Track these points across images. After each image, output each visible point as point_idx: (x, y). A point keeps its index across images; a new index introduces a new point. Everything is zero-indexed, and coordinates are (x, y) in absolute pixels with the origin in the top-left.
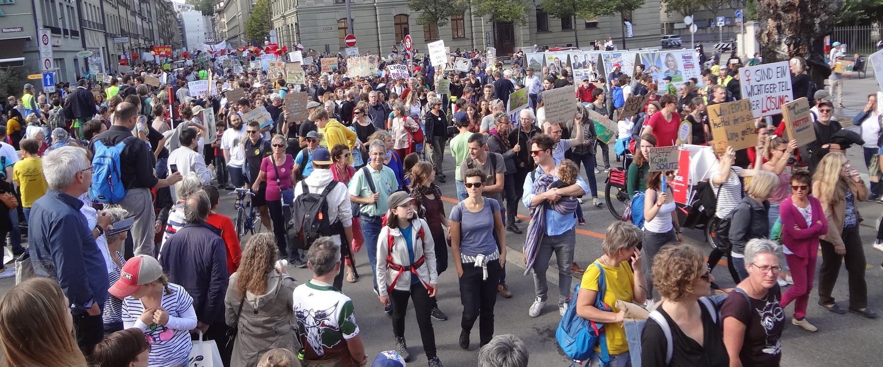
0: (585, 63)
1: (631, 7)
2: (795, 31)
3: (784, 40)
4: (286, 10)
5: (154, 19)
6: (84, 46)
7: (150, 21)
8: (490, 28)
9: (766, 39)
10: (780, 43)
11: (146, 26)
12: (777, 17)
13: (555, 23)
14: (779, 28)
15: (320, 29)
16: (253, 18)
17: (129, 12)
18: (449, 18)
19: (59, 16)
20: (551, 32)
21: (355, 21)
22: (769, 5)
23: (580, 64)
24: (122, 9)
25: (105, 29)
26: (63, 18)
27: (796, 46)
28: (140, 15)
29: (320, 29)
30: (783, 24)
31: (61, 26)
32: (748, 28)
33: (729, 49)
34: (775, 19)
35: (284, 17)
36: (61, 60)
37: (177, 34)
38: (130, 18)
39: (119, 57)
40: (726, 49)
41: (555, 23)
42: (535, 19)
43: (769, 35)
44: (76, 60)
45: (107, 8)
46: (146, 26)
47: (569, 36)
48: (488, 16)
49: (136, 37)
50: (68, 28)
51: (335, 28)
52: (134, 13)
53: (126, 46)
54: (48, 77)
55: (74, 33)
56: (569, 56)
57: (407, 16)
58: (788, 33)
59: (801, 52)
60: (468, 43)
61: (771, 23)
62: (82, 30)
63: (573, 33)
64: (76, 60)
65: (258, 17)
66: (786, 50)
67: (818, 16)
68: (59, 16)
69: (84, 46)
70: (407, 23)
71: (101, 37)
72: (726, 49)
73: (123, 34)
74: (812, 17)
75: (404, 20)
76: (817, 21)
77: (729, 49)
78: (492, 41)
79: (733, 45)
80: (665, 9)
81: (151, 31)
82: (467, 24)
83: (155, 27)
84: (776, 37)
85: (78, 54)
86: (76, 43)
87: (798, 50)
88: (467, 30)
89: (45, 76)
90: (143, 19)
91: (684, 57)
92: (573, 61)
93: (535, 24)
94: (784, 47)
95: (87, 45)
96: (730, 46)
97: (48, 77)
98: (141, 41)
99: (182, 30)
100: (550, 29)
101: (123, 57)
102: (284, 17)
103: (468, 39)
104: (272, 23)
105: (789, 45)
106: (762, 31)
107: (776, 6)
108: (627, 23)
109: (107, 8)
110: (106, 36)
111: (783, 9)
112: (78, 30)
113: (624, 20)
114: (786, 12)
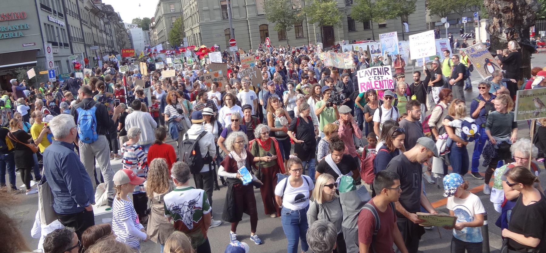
0: (378, 50)
1: (407, 13)
2: (511, 25)
3: (504, 30)
4: (193, 25)
5: (113, 34)
6: (72, 52)
7: (111, 36)
8: (319, 31)
9: (493, 30)
10: (501, 33)
11: (109, 38)
12: (499, 16)
13: (359, 25)
14: (500, 23)
16: (173, 31)
18: (293, 25)
19: (56, 35)
20: (357, 31)
21: (235, 30)
22: (494, 9)
23: (375, 51)
24: (94, 29)
26: (59, 36)
27: (512, 34)
28: (105, 32)
30: (503, 20)
31: (58, 41)
32: (482, 23)
33: (470, 37)
34: (498, 18)
35: (192, 29)
36: (59, 61)
37: (128, 42)
38: (99, 34)
39: (94, 58)
40: (469, 37)
41: (359, 25)
42: (347, 24)
43: (494, 28)
44: (68, 61)
45: (85, 29)
46: (109, 38)
47: (368, 33)
48: (318, 23)
49: (103, 45)
50: (62, 42)
51: (223, 34)
52: (101, 31)
53: (98, 51)
54: (52, 72)
55: (66, 45)
56: (368, 46)
57: (267, 25)
58: (506, 26)
59: (515, 37)
60: (305, 40)
61: (495, 20)
62: (70, 43)
63: (371, 32)
64: (68, 61)
65: (176, 30)
66: (506, 37)
67: (525, 14)
68: (56, 35)
69: (72, 52)
71: (82, 46)
72: (469, 37)
73: (95, 44)
74: (522, 15)
75: (265, 27)
76: (525, 18)
77: (470, 37)
78: (320, 38)
79: (473, 34)
80: (429, 13)
81: (112, 42)
82: (304, 29)
83: (114, 39)
84: (499, 29)
85: (69, 58)
86: (67, 51)
87: (513, 37)
88: (305, 32)
89: (50, 71)
90: (107, 34)
91: (441, 44)
92: (371, 49)
93: (347, 27)
94: (504, 35)
95: (74, 52)
96: (471, 35)
97: (52, 72)
98: (106, 48)
99: (131, 40)
101: (96, 58)
102: (192, 29)
103: (305, 38)
104: (185, 33)
105: (507, 34)
106: (490, 26)
107: (498, 9)
108: (405, 24)
109: (85, 29)
110: (85, 46)
111: (503, 11)
112: (68, 43)
113: (403, 22)
114: (505, 13)
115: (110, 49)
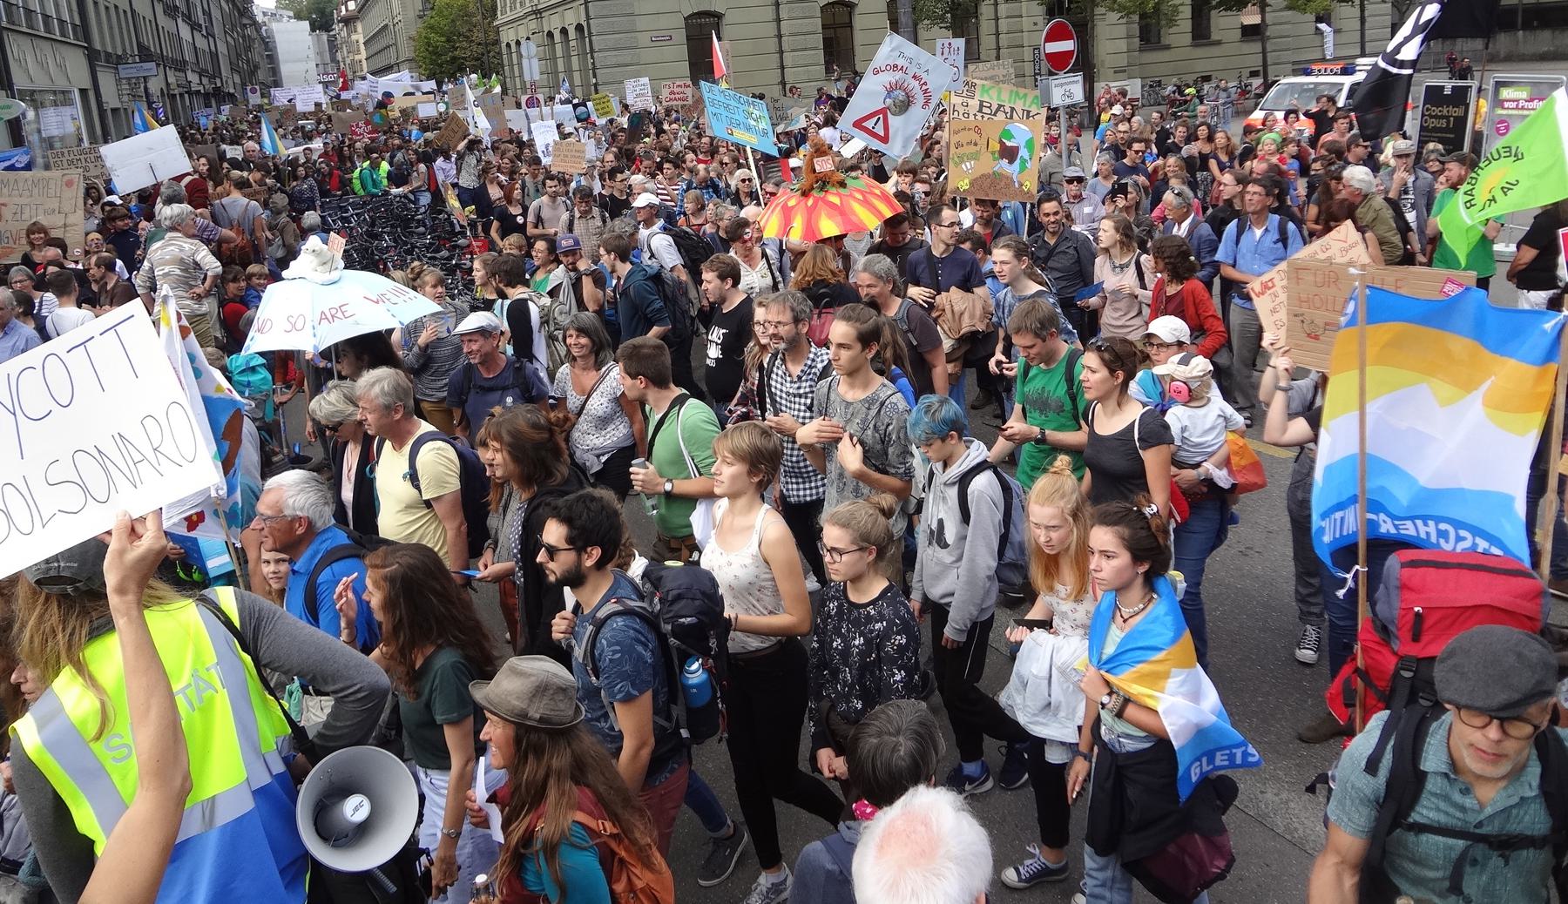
5: (217, 30)
7: (210, 35)
11: (201, 43)
15: (644, 39)
16: (431, 28)
17: (159, 8)
20: (1168, 47)
25: (87, 37)
29: (644, 39)
38: (163, 21)
46: (201, 43)
49: (180, 66)
51: (681, 37)
53: (155, 86)
70: (850, 25)
81: (214, 56)
83: (222, 48)
90: (195, 27)
98: (193, 77)
100: (1215, 37)
110: (92, 57)
115: (205, 81)
